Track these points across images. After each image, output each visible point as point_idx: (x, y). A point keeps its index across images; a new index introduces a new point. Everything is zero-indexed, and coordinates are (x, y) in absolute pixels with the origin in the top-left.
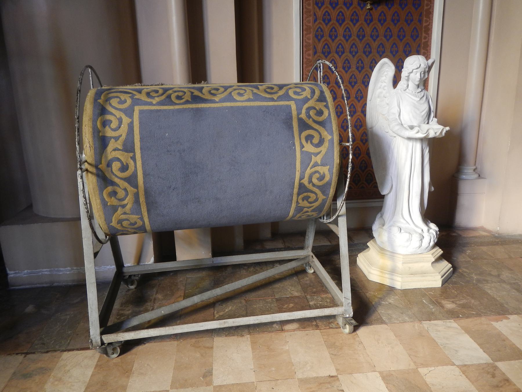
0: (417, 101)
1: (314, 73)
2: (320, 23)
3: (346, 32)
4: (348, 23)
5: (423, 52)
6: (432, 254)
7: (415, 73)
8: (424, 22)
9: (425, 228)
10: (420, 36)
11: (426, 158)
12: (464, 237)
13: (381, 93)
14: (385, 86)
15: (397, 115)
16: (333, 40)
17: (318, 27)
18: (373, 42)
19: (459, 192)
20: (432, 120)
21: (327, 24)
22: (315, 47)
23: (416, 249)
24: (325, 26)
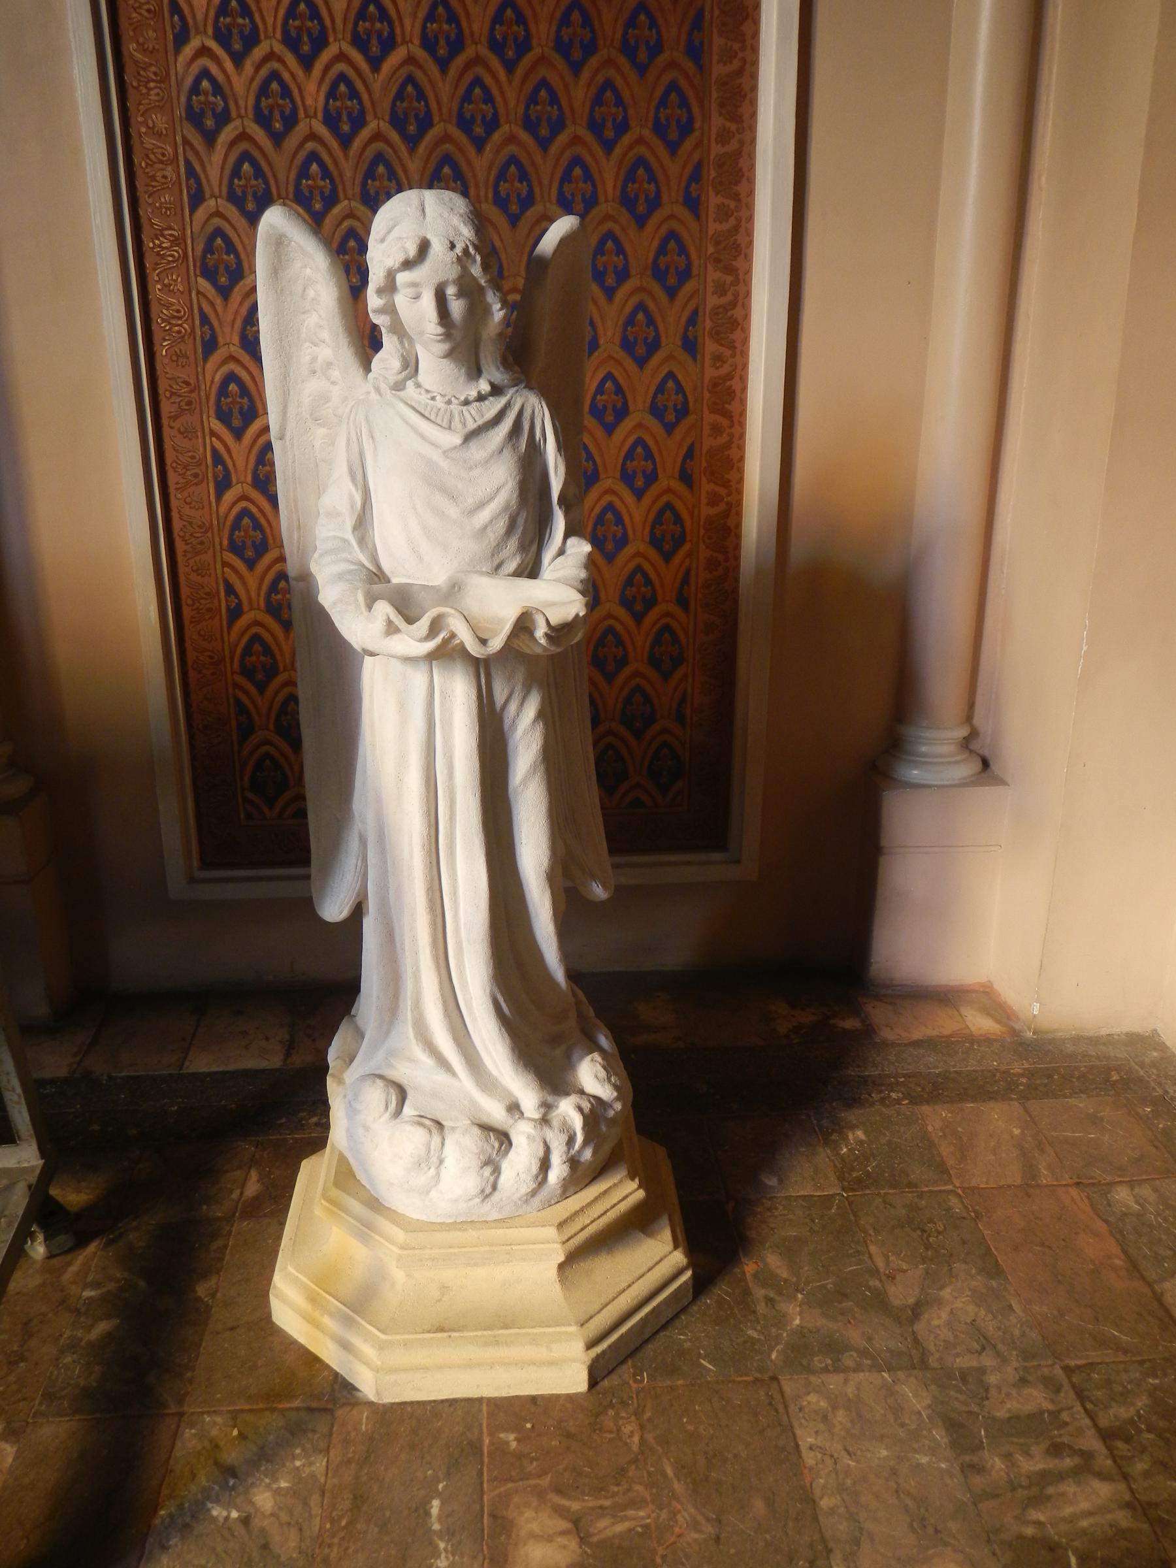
0: (444, 452)
1: (198, 292)
2: (203, 51)
3: (335, 99)
4: (341, 57)
5: (718, 206)
6: (561, 1225)
7: (411, 291)
8: (715, 58)
9: (528, 1096)
10: (697, 125)
11: (520, 748)
12: (885, 1044)
13: (324, 398)
14: (329, 364)
15: (349, 523)
16: (278, 139)
17: (195, 69)
18: (471, 150)
19: (884, 842)
20: (561, 552)
21: (238, 59)
22: (191, 172)
23: (472, 1203)
24: (229, 65)
